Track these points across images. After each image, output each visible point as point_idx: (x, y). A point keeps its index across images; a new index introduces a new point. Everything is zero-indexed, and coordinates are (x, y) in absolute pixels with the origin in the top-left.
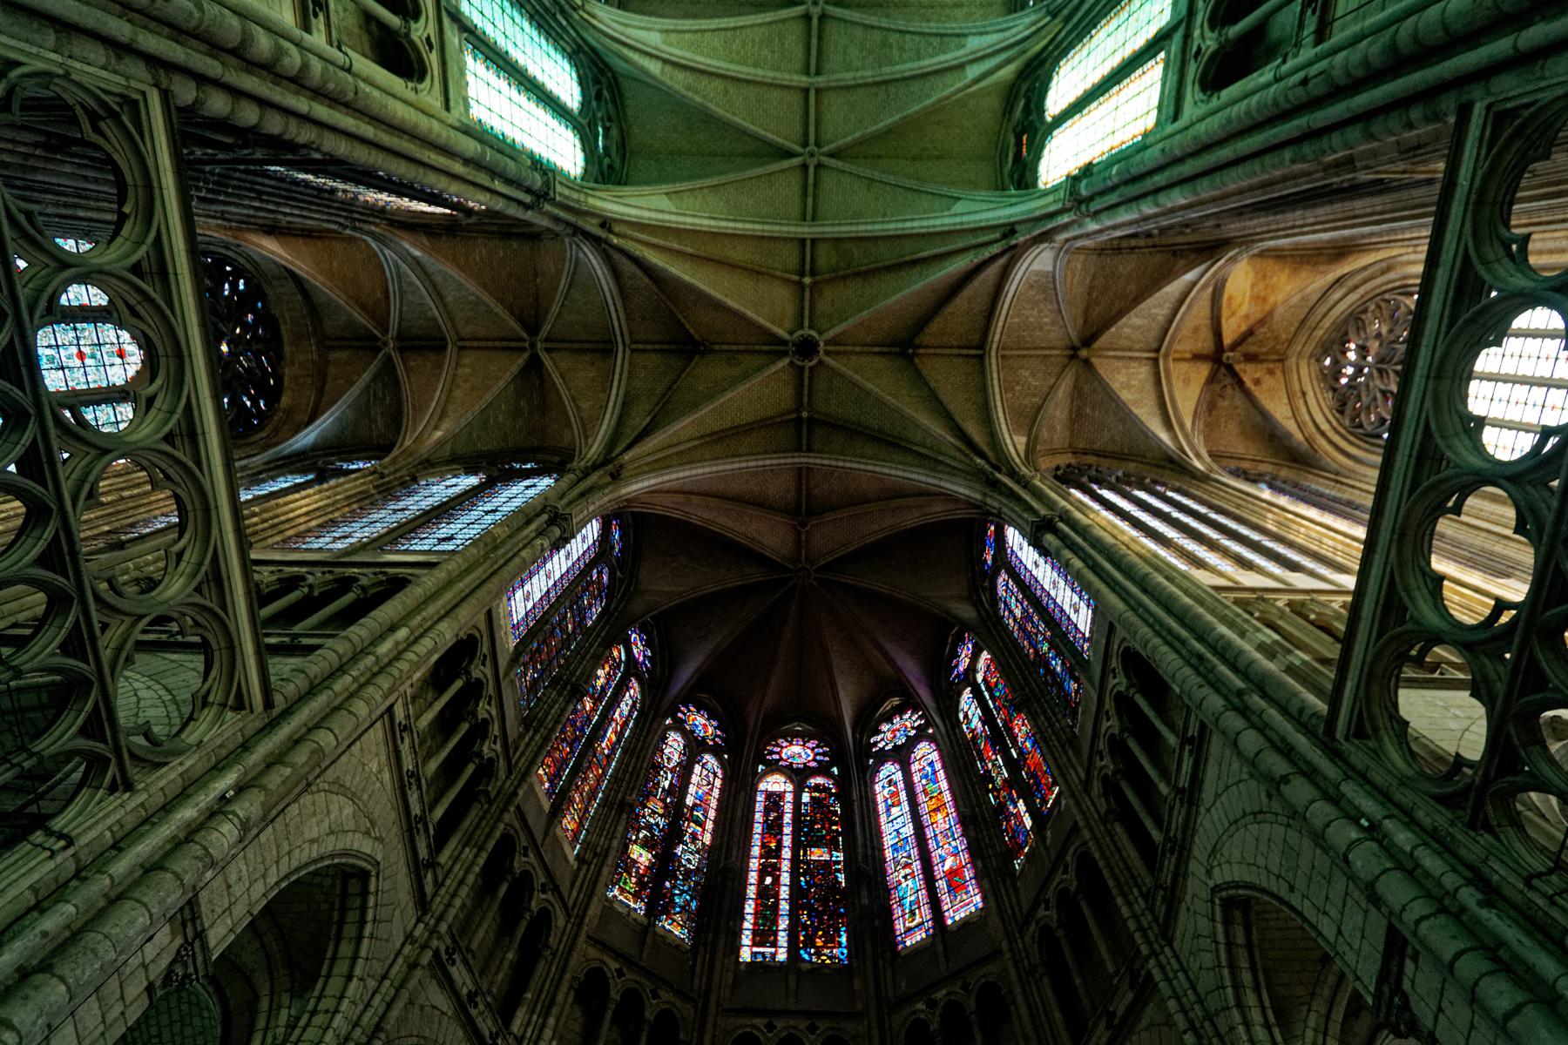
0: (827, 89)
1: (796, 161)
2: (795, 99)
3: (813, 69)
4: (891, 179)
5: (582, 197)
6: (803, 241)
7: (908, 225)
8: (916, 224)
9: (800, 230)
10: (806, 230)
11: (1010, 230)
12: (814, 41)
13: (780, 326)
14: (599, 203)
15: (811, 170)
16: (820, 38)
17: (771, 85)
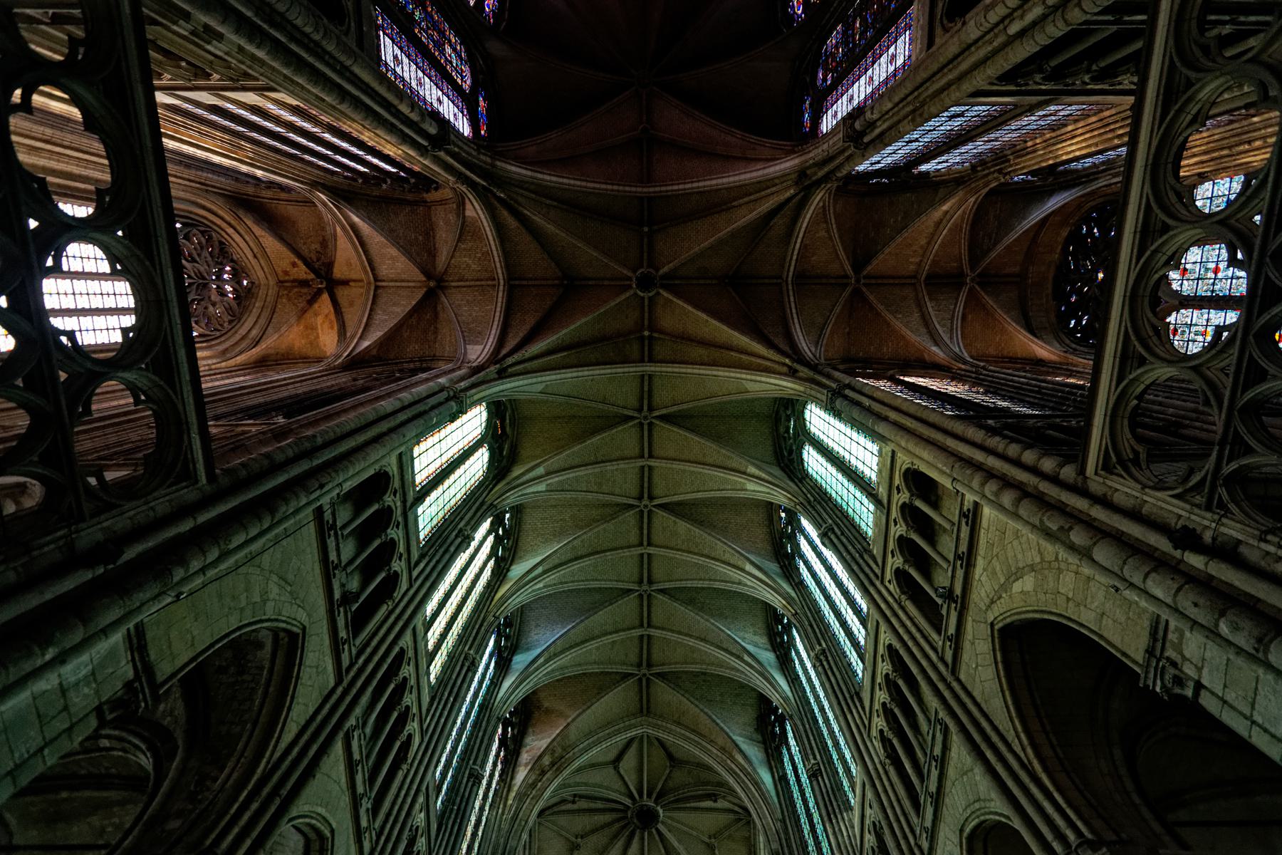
0: (635, 458)
1: (657, 413)
2: (657, 452)
3: (646, 469)
4: (589, 404)
5: (808, 391)
6: (651, 360)
7: (575, 374)
8: (569, 375)
9: (653, 369)
10: (648, 368)
11: (502, 375)
12: (646, 485)
13: (667, 299)
14: (797, 387)
15: (645, 408)
16: (642, 486)
17: (675, 460)
